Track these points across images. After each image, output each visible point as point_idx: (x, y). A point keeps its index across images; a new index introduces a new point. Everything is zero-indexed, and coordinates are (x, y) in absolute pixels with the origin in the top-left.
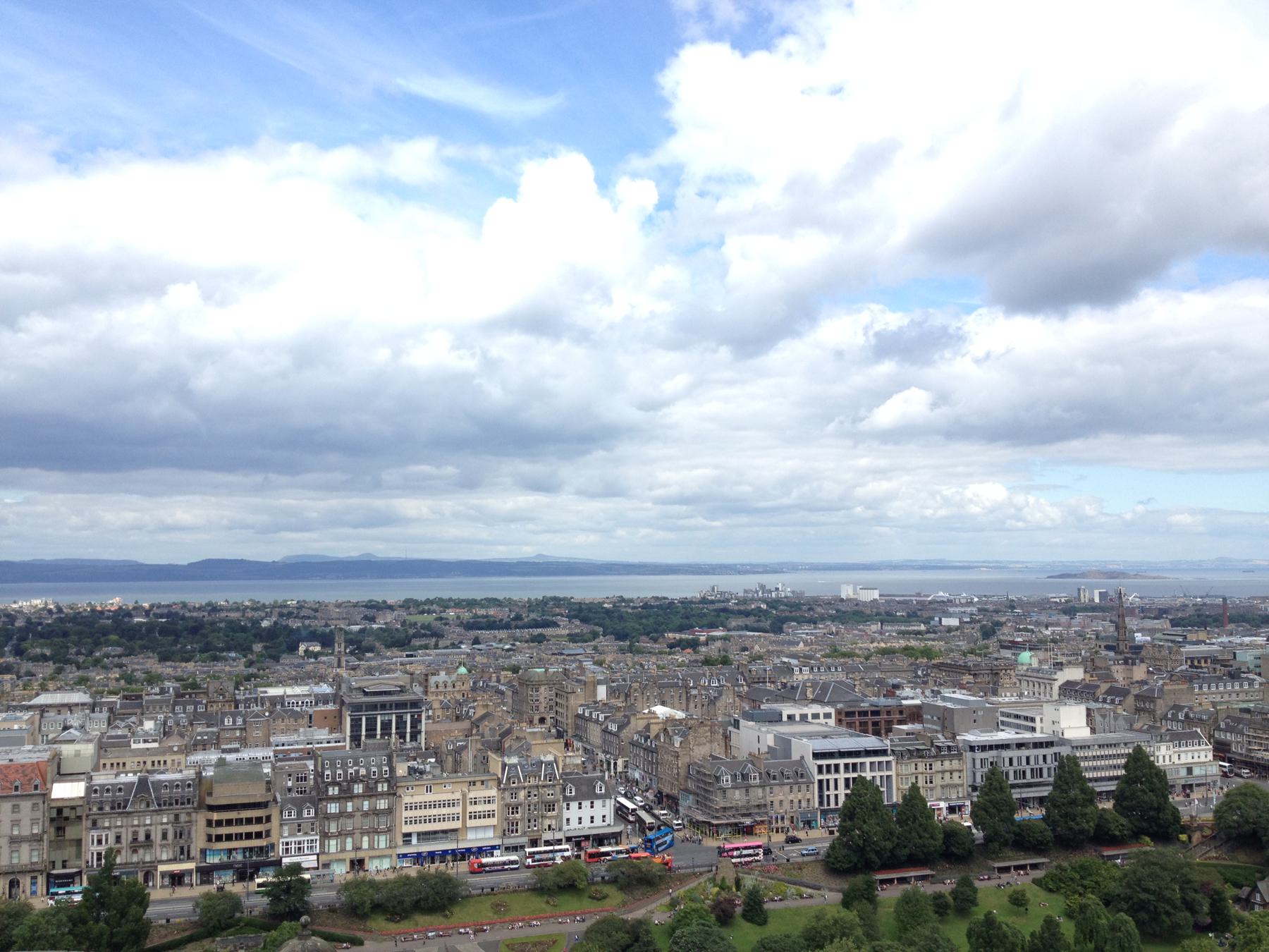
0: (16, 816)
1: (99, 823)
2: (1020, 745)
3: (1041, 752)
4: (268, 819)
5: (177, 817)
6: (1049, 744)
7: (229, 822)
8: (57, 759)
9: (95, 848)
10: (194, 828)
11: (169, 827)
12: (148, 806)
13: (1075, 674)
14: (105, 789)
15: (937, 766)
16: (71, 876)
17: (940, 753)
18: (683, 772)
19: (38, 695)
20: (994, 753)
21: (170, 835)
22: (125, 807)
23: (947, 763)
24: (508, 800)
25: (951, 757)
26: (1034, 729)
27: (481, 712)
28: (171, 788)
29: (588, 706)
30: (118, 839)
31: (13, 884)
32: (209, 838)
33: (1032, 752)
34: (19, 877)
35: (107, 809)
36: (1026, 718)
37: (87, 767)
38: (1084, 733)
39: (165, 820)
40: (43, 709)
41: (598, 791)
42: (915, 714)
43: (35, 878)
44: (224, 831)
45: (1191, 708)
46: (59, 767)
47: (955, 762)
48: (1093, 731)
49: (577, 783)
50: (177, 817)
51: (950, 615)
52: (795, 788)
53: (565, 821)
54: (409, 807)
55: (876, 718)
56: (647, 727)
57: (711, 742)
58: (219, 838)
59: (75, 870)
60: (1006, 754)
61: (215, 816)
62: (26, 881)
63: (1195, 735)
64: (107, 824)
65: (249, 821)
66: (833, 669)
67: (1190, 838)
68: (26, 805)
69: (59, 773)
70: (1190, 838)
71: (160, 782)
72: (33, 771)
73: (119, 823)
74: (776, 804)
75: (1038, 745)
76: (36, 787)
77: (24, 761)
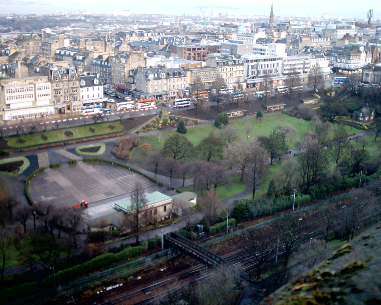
2: (265, 60)
3: (272, 62)
6: (275, 60)
13: (262, 34)
15: (234, 68)
17: (235, 64)
18: (127, 75)
20: (255, 63)
23: (238, 67)
24: (55, 88)
25: (239, 64)
26: (264, 54)
27: (13, 52)
29: (62, 49)
33: (269, 63)
36: (261, 50)
38: (284, 55)
41: (95, 83)
42: (215, 49)
45: (313, 47)
47: (241, 67)
48: (288, 55)
49: (85, 79)
51: (167, 21)
52: (180, 79)
53: (81, 97)
54: (10, 92)
55: (199, 51)
56: (100, 57)
57: (139, 61)
60: (260, 63)
63: (322, 57)
66: (161, 34)
67: (331, 94)
70: (331, 94)
74: (172, 87)
75: (271, 60)
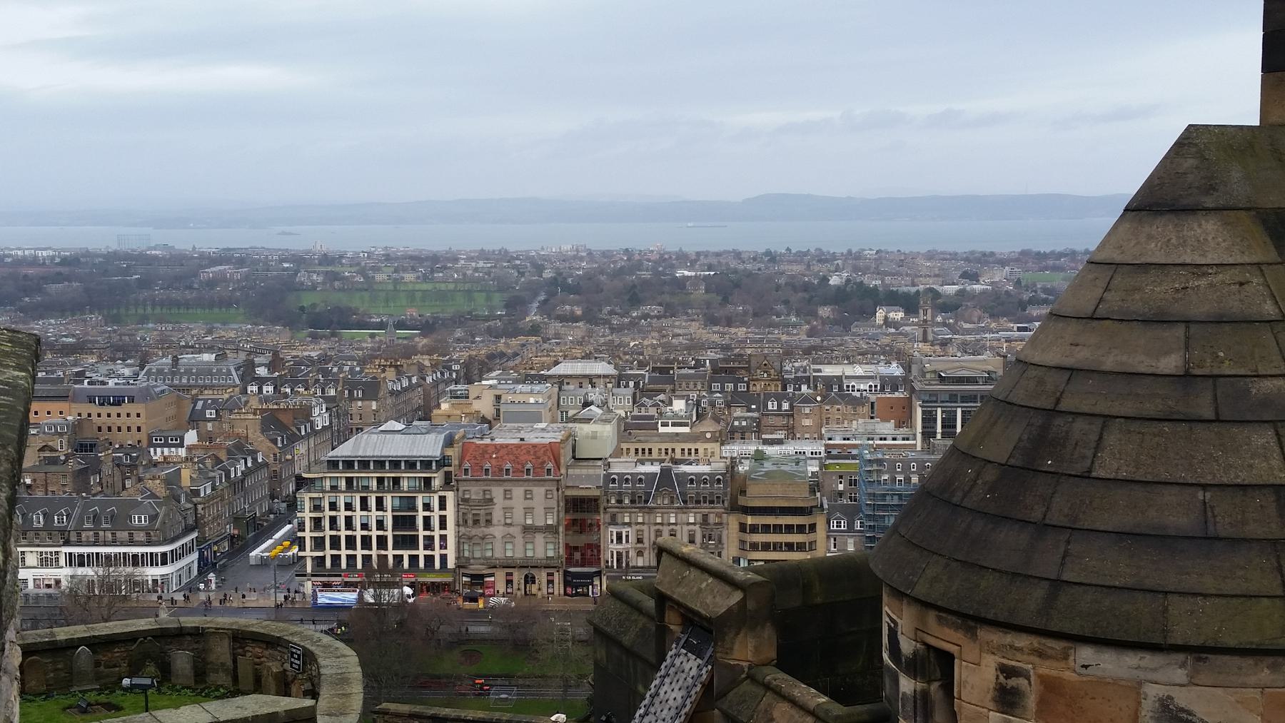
0: (529, 503)
1: (619, 521)
4: (813, 527)
5: (705, 517)
7: (766, 529)
8: (572, 440)
9: (615, 547)
10: (725, 533)
11: (697, 527)
12: (672, 502)
14: (623, 478)
16: (590, 576)
21: (698, 538)
22: (646, 502)
28: (698, 483)
30: (640, 541)
31: (529, 580)
32: (743, 542)
34: (534, 572)
35: (627, 501)
37: (607, 451)
39: (692, 520)
43: (552, 574)
44: (760, 538)
46: (574, 451)
50: (705, 517)
58: (754, 547)
59: (594, 570)
61: (750, 520)
62: (542, 576)
64: (627, 520)
65: (789, 529)
68: (539, 491)
69: (574, 457)
71: (685, 474)
72: (545, 452)
73: (640, 520)
76: (549, 470)
77: (536, 441)
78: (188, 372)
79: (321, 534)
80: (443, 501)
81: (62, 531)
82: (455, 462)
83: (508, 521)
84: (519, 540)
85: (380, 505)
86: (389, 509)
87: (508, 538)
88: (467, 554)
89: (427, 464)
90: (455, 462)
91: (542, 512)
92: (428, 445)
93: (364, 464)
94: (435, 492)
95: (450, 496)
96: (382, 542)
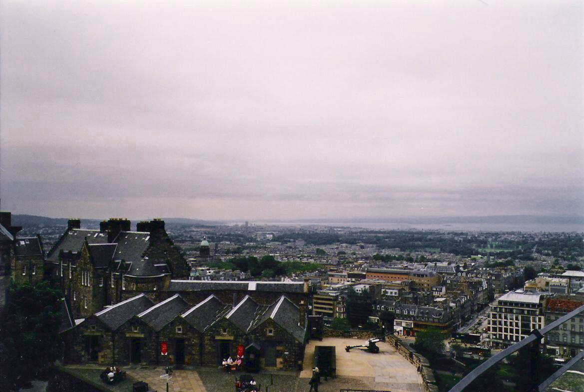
19: (565, 272)
40: (570, 278)
78: (440, 267)
79: (496, 326)
80: (540, 319)
81: (413, 316)
82: (544, 305)
83: (565, 329)
84: (569, 336)
85: (517, 319)
86: (520, 320)
87: (565, 335)
88: (548, 339)
89: (534, 305)
90: (544, 305)
91: (578, 327)
92: (535, 299)
93: (511, 303)
94: (537, 316)
95: (543, 317)
96: (517, 332)
